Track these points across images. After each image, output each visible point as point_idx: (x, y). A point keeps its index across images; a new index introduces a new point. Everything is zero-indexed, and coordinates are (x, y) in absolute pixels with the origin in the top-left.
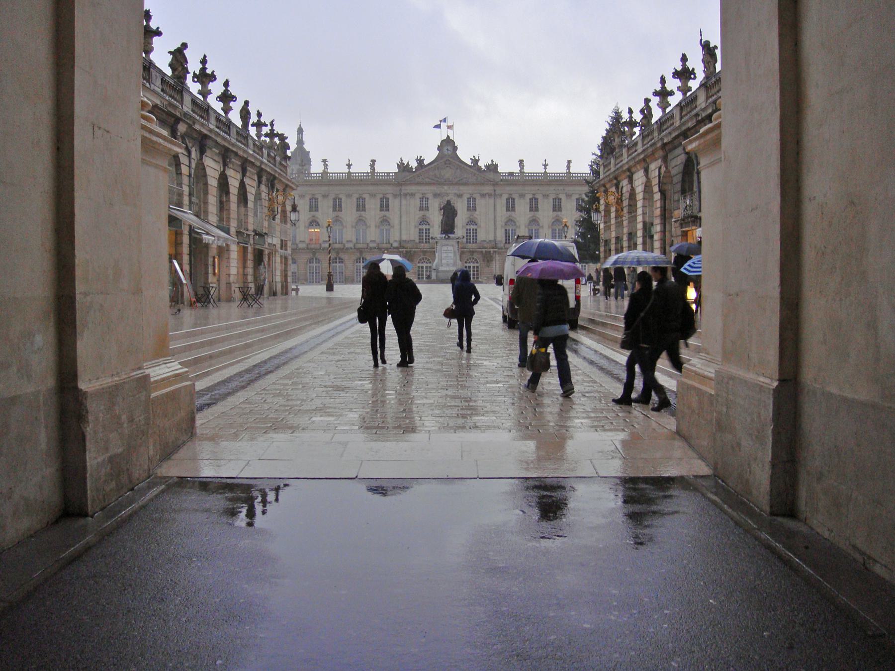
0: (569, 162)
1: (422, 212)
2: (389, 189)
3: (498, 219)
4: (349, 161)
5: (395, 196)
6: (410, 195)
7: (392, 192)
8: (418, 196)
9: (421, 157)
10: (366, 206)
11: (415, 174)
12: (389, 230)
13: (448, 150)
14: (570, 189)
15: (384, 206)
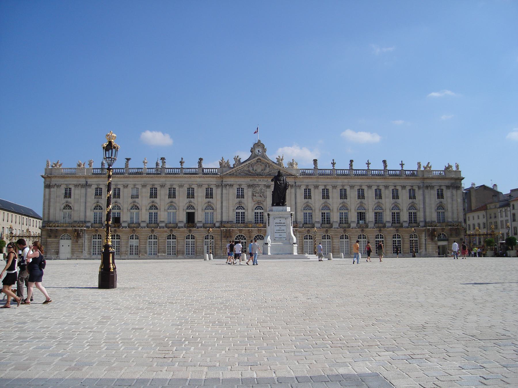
0: (351, 161)
1: (239, 199)
2: (213, 181)
3: (298, 205)
4: (182, 159)
5: (217, 186)
6: (229, 185)
7: (215, 183)
8: (236, 187)
9: (238, 156)
10: (195, 194)
11: (233, 170)
12: (213, 213)
13: (259, 151)
14: (352, 182)
15: (209, 195)
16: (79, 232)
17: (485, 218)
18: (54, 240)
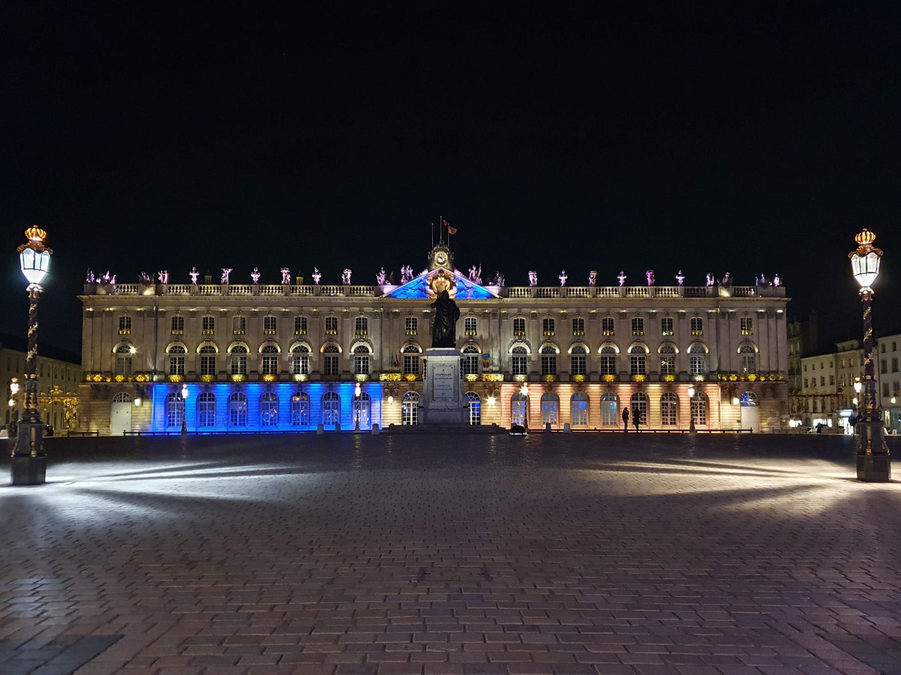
16: (145, 390)
17: (834, 366)
18: (103, 403)
